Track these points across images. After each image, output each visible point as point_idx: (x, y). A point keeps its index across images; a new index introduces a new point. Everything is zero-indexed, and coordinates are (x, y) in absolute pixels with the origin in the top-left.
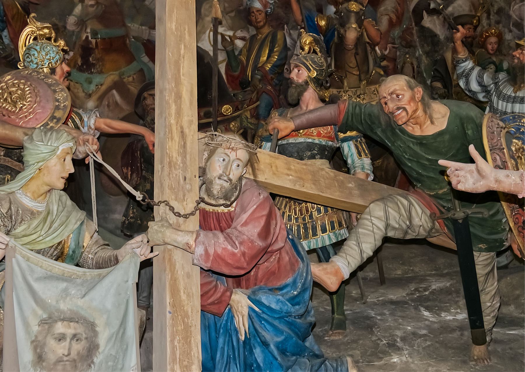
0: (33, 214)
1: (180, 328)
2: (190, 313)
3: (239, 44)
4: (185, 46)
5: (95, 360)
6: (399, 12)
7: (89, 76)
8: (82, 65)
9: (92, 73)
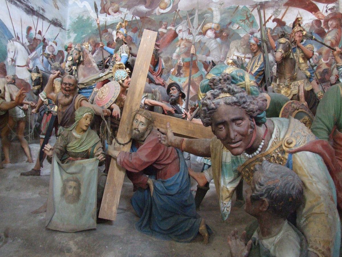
3: (247, 60)
4: (142, 71)
6: (338, 37)
8: (177, 74)
9: (181, 77)
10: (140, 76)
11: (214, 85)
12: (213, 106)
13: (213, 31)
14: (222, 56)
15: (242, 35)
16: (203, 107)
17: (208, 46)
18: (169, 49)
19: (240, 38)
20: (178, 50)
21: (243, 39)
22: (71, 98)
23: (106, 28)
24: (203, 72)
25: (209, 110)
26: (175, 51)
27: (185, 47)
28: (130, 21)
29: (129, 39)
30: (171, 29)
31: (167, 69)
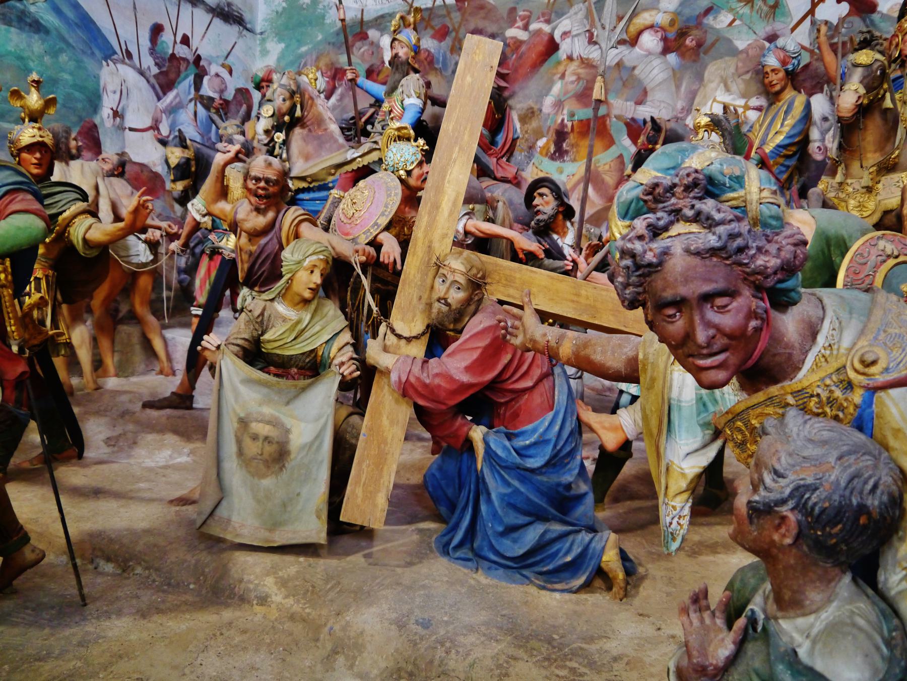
0: (285, 320)
1: (372, 453)
2: (389, 440)
3: (753, 115)
4: (460, 148)
5: (286, 465)
7: (562, 165)
8: (555, 152)
9: (564, 161)
10: (455, 162)
11: (657, 201)
12: (650, 257)
13: (659, 34)
14: (680, 105)
15: (741, 45)
16: (621, 258)
17: (642, 76)
18: (533, 85)
19: (734, 52)
20: (557, 88)
21: (744, 55)
22: (271, 215)
23: (365, 28)
24: (626, 148)
25: (638, 267)
26: (550, 89)
27: (579, 79)
28: (427, 9)
29: (426, 59)
30: (539, 32)
31: (527, 140)
